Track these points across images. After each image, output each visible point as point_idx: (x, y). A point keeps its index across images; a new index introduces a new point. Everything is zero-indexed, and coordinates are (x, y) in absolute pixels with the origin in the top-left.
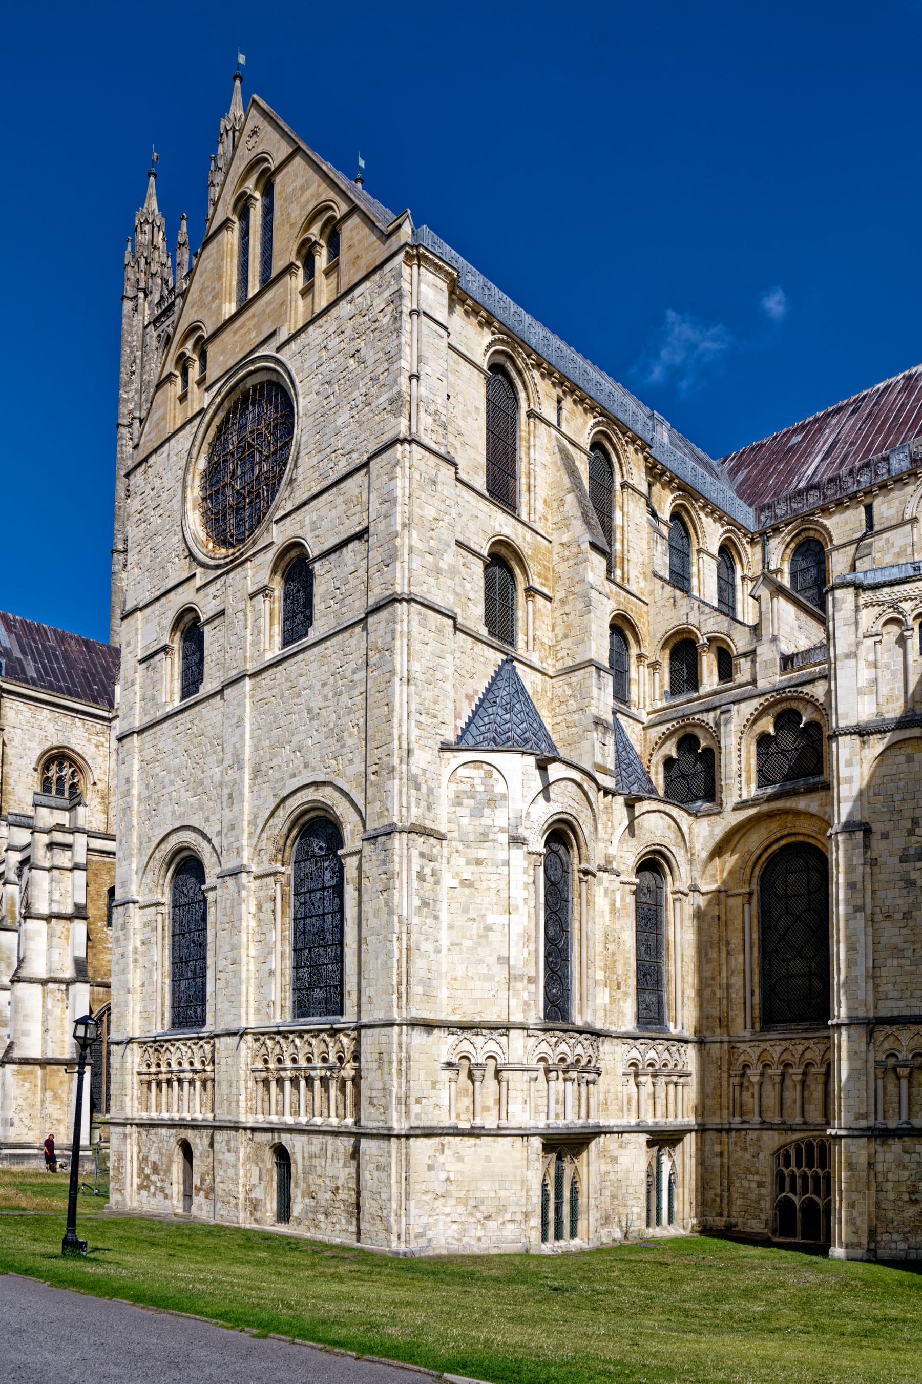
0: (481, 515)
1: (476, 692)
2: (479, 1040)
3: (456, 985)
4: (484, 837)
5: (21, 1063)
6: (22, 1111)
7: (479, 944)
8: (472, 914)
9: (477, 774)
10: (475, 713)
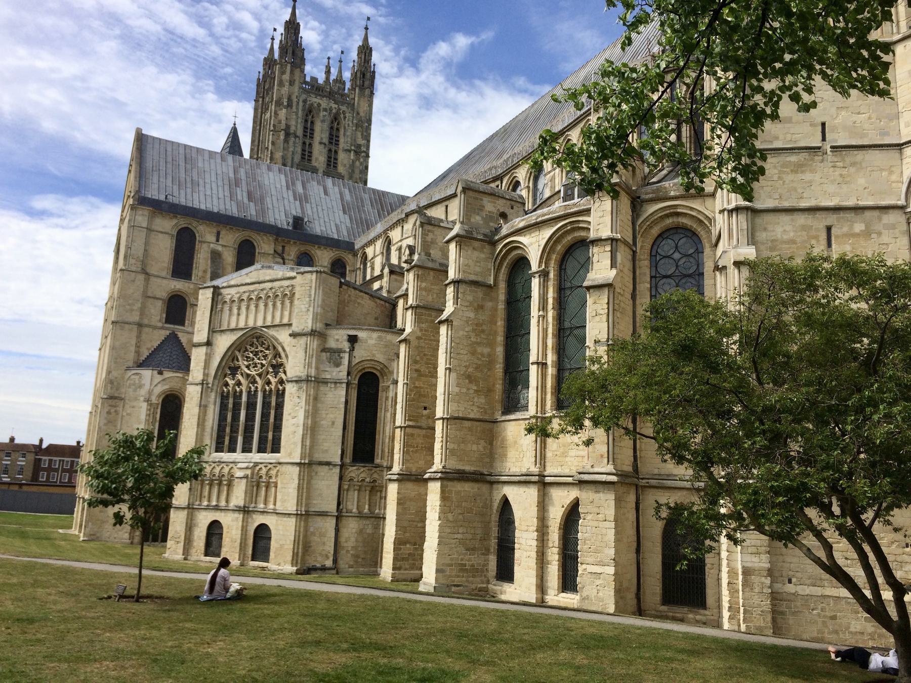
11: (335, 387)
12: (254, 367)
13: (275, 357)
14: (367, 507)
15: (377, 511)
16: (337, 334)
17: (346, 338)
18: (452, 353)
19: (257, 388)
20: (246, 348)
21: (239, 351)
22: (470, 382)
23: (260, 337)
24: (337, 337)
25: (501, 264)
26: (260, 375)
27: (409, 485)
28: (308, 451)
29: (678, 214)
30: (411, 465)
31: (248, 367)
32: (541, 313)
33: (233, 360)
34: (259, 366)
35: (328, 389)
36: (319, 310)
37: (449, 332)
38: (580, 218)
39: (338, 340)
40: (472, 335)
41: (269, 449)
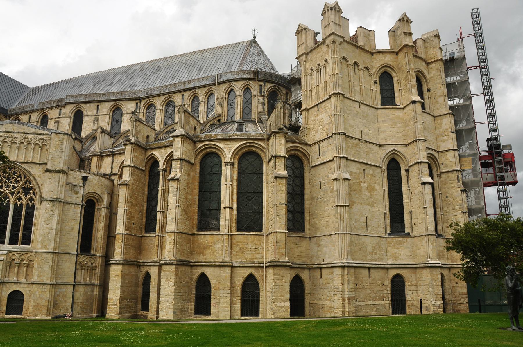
11: (75, 207)
12: (6, 187)
13: (26, 183)
14: (88, 279)
15: (93, 281)
17: (80, 177)
18: (178, 197)
19: (9, 201)
22: (185, 213)
24: (75, 176)
25: (199, 153)
26: (12, 194)
27: (126, 267)
28: (58, 245)
29: (296, 150)
30: (127, 256)
32: (231, 183)
34: (11, 187)
35: (70, 207)
36: (67, 159)
37: (178, 186)
38: (256, 142)
40: (186, 188)
41: (19, 242)
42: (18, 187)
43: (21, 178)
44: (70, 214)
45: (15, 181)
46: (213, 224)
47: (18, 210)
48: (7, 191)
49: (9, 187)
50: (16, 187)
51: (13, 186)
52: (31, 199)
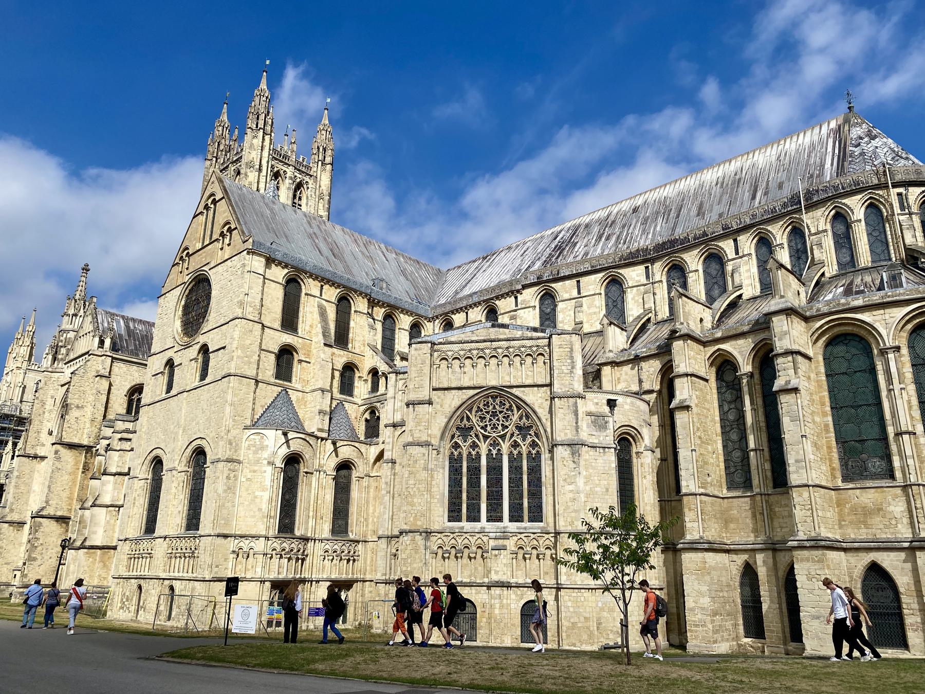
0: (276, 337)
1: (266, 404)
2: (248, 541)
3: (241, 519)
4: (258, 462)
5: (89, 549)
6: (86, 573)
7: (251, 503)
8: (250, 492)
9: (257, 437)
10: (264, 412)
11: (604, 452)
13: (521, 418)
16: (595, 398)
20: (479, 407)
21: (470, 411)
23: (497, 397)
31: (484, 428)
33: (462, 420)
34: (500, 428)
35: (597, 454)
39: (597, 404)
42: (510, 427)
43: (512, 411)
44: (600, 464)
45: (504, 417)
46: (874, 467)
47: (515, 464)
48: (494, 435)
49: (497, 428)
50: (507, 427)
51: (502, 425)
52: (534, 444)
